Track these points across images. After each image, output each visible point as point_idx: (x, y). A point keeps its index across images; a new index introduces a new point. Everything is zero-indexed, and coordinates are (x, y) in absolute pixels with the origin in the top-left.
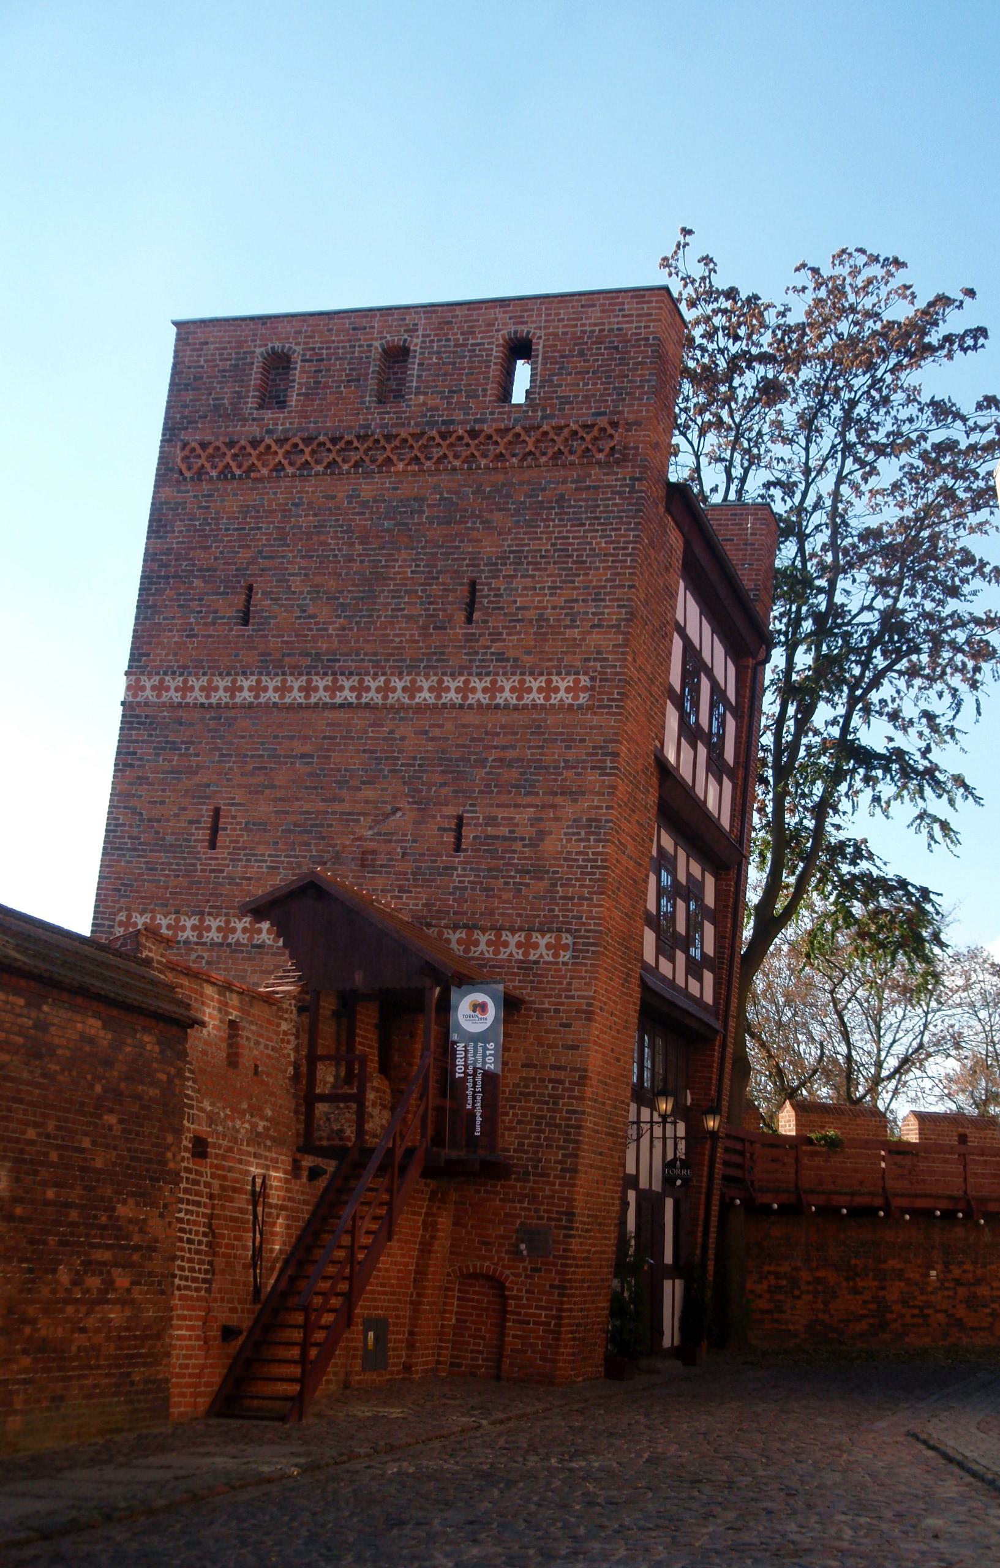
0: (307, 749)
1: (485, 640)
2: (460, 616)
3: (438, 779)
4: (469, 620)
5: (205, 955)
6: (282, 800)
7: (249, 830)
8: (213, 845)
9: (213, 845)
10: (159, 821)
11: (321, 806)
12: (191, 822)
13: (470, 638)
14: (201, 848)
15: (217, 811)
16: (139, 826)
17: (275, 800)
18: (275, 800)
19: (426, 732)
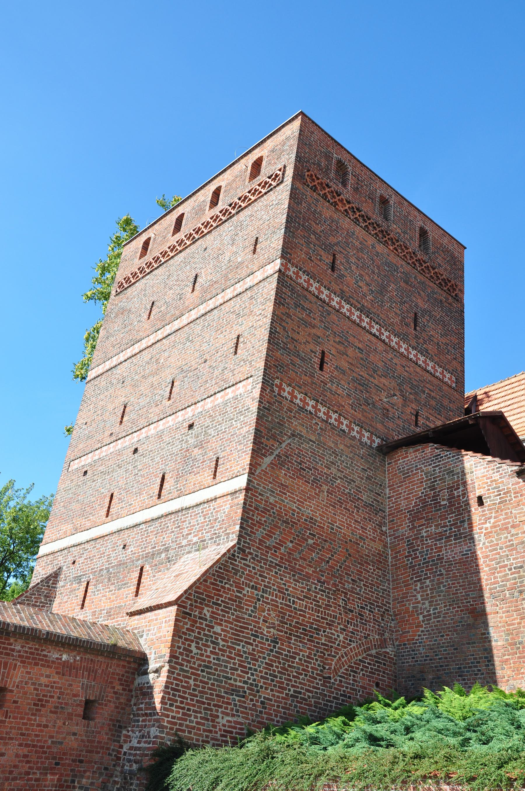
0: (360, 346)
1: (421, 340)
2: (412, 325)
3: (409, 390)
4: (415, 329)
5: (320, 423)
6: (351, 364)
7: (338, 371)
8: (321, 368)
9: (321, 368)
10: (297, 341)
11: (366, 375)
12: (312, 351)
13: (416, 336)
14: (317, 366)
15: (323, 353)
16: (286, 338)
17: (348, 362)
18: (348, 362)
19: (404, 367)
